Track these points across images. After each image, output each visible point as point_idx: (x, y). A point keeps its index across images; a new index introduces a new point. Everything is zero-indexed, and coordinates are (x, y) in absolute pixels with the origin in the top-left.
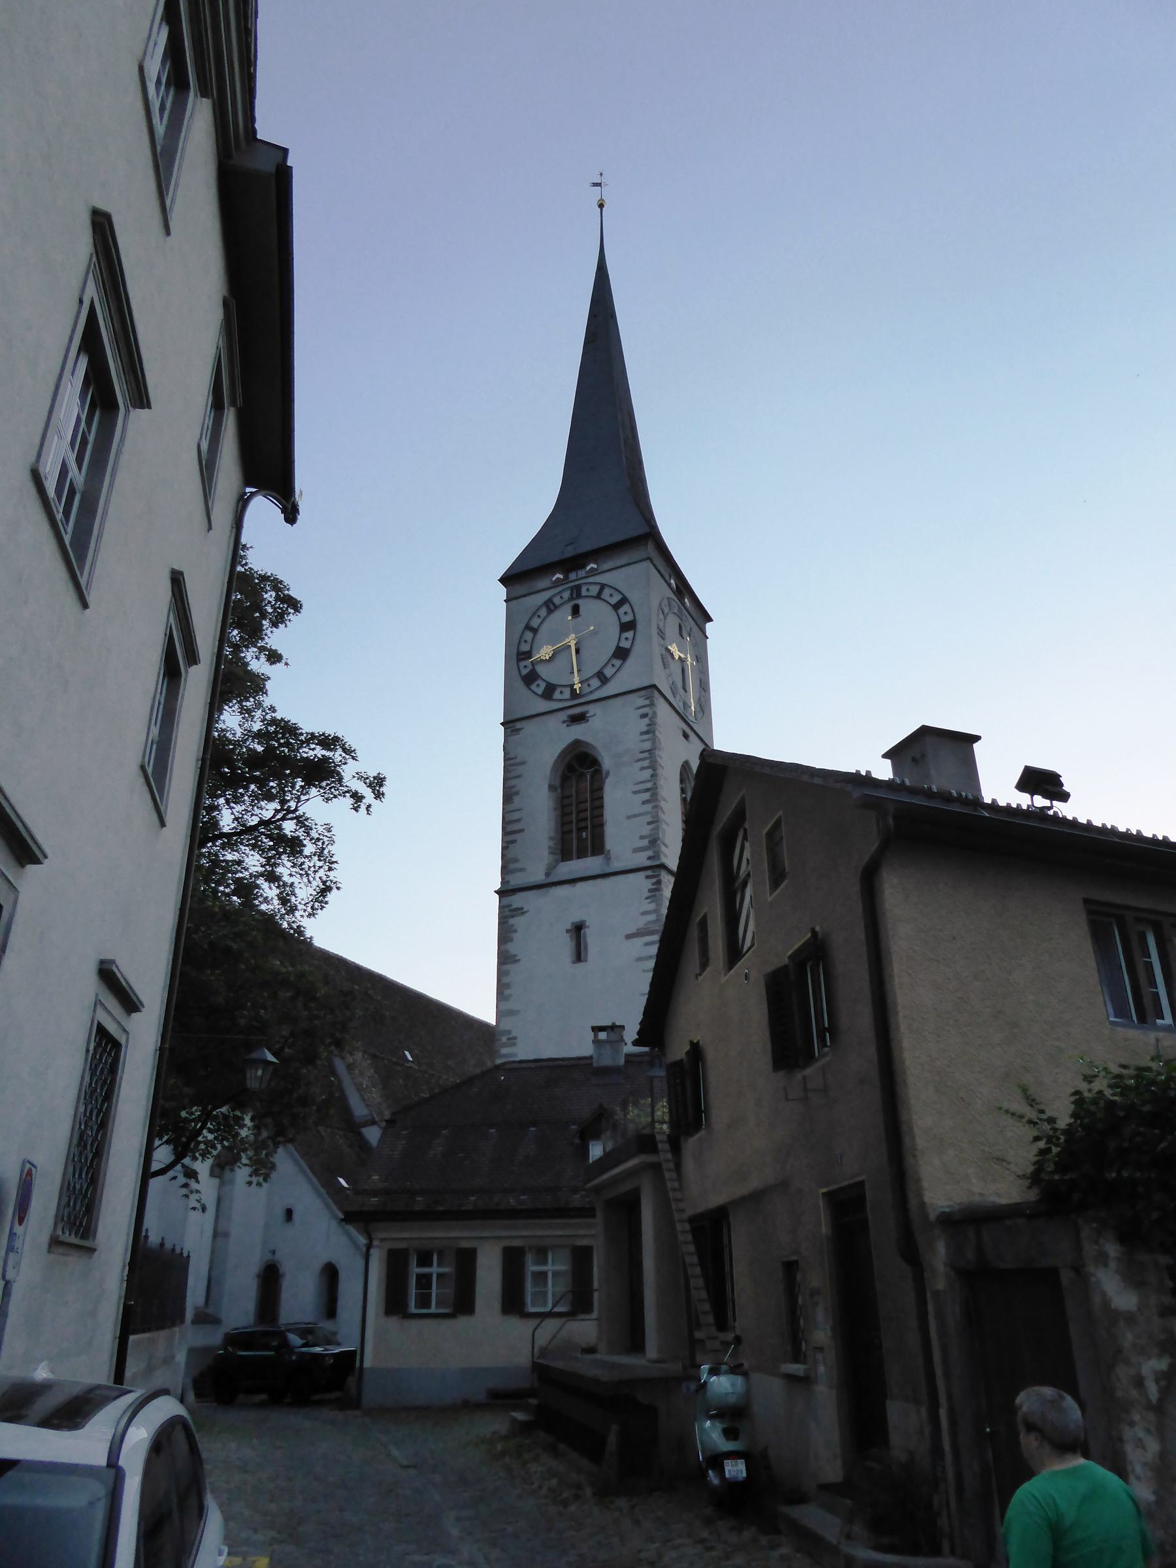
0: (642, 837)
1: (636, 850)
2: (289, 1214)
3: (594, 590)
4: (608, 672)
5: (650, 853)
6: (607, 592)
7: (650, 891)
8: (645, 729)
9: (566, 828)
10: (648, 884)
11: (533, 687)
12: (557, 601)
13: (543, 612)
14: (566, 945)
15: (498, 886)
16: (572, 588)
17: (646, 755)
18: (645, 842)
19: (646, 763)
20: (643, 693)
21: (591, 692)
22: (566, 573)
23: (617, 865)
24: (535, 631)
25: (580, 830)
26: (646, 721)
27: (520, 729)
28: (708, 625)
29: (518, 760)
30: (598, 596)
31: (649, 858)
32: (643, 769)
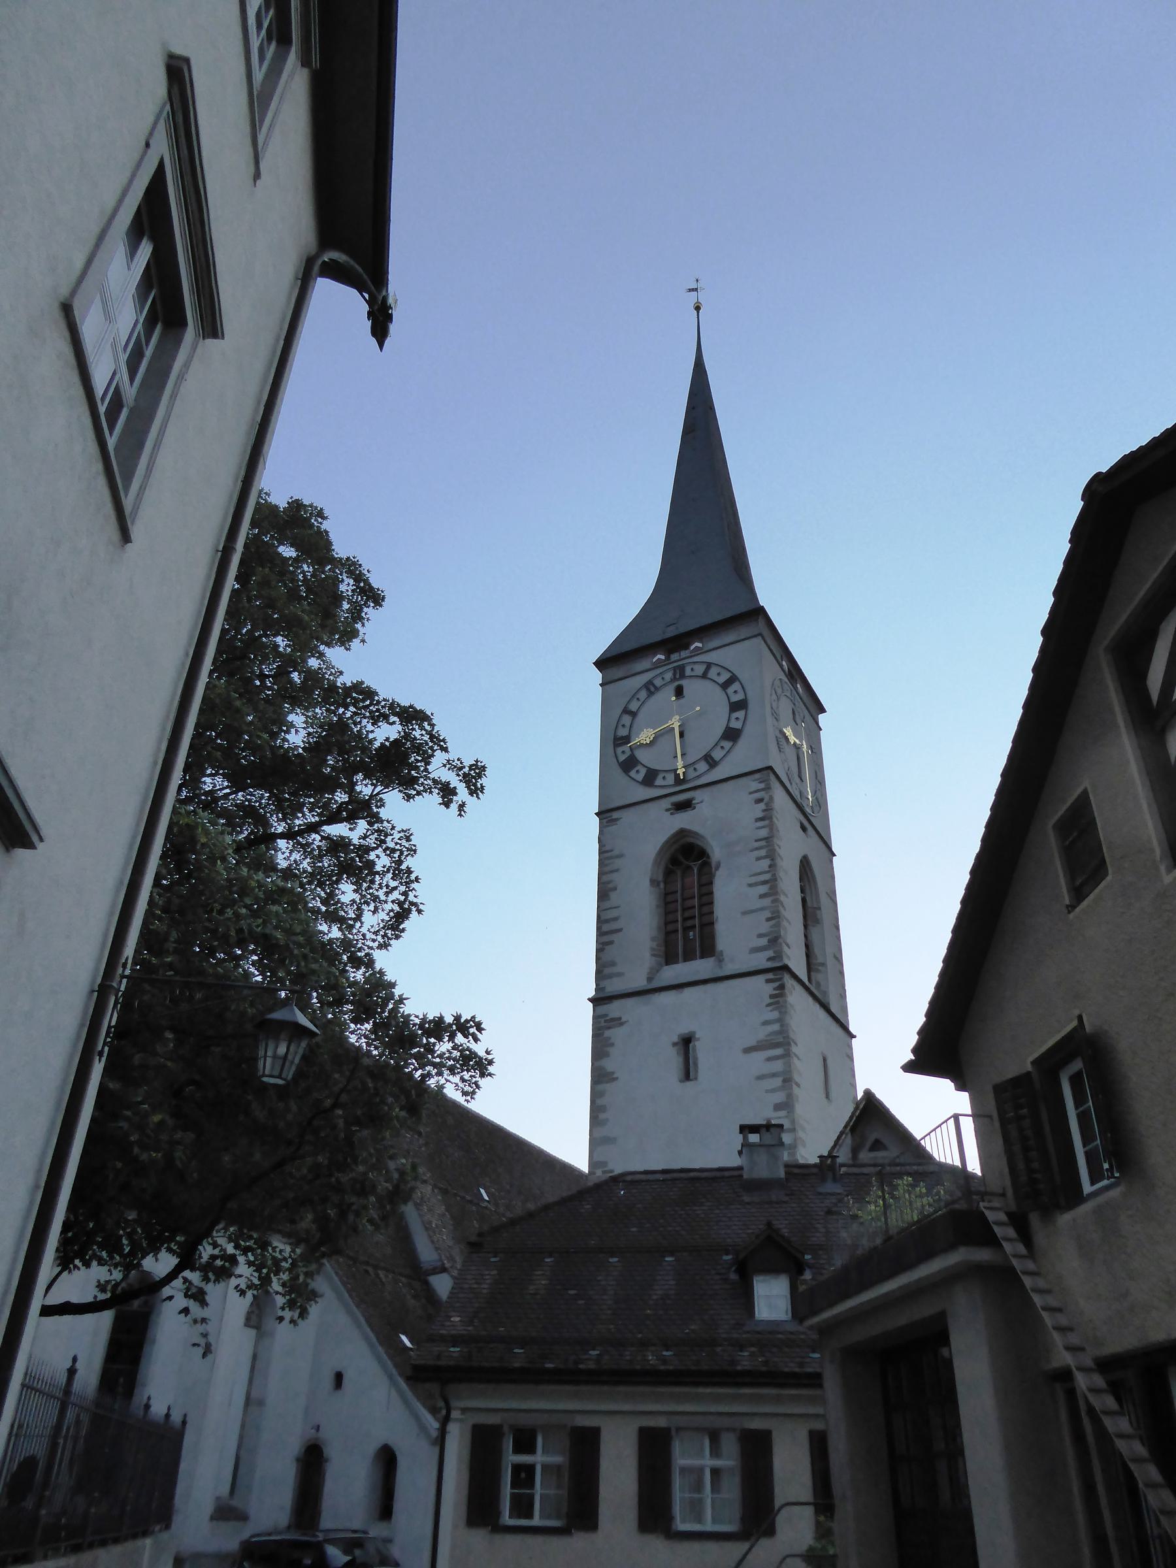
0: (760, 936)
2: (339, 1378)
3: (700, 670)
4: (717, 755)
5: (770, 953)
6: (713, 673)
7: (771, 996)
8: (761, 815)
9: (671, 927)
10: (769, 989)
11: (633, 773)
12: (658, 682)
13: (643, 694)
14: (674, 1059)
15: (592, 993)
16: (675, 669)
17: (763, 843)
18: (764, 941)
19: (763, 853)
20: (757, 776)
21: (698, 777)
22: (668, 653)
23: (729, 969)
24: (633, 714)
25: (686, 929)
26: (762, 806)
27: (616, 820)
28: (821, 717)
29: (616, 852)
30: (704, 676)
32: (758, 859)
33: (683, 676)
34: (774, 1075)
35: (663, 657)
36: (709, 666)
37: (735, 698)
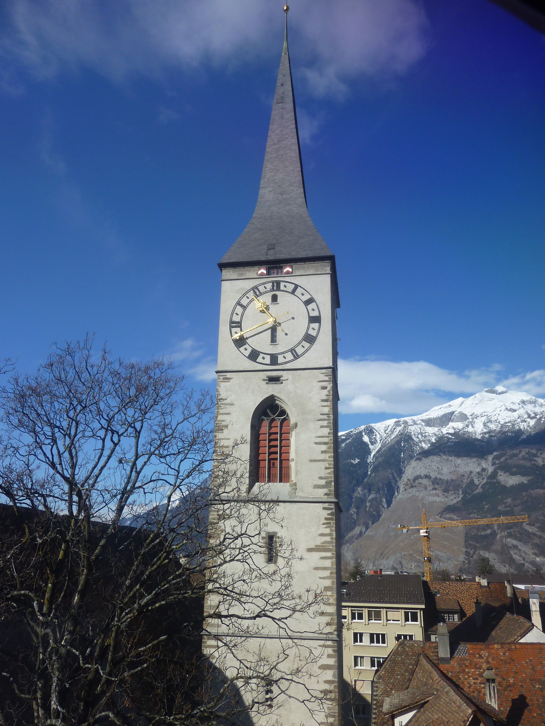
0: (321, 478)
1: (317, 487)
3: (291, 287)
4: (299, 350)
6: (299, 291)
7: (326, 519)
8: (325, 398)
11: (242, 349)
12: (261, 288)
16: (273, 282)
17: (325, 417)
20: (324, 371)
21: (286, 363)
23: (300, 495)
24: (244, 308)
27: (230, 379)
31: (326, 494)
32: (322, 427)
33: (278, 289)
34: (325, 569)
35: (265, 272)
36: (296, 286)
37: (313, 314)
